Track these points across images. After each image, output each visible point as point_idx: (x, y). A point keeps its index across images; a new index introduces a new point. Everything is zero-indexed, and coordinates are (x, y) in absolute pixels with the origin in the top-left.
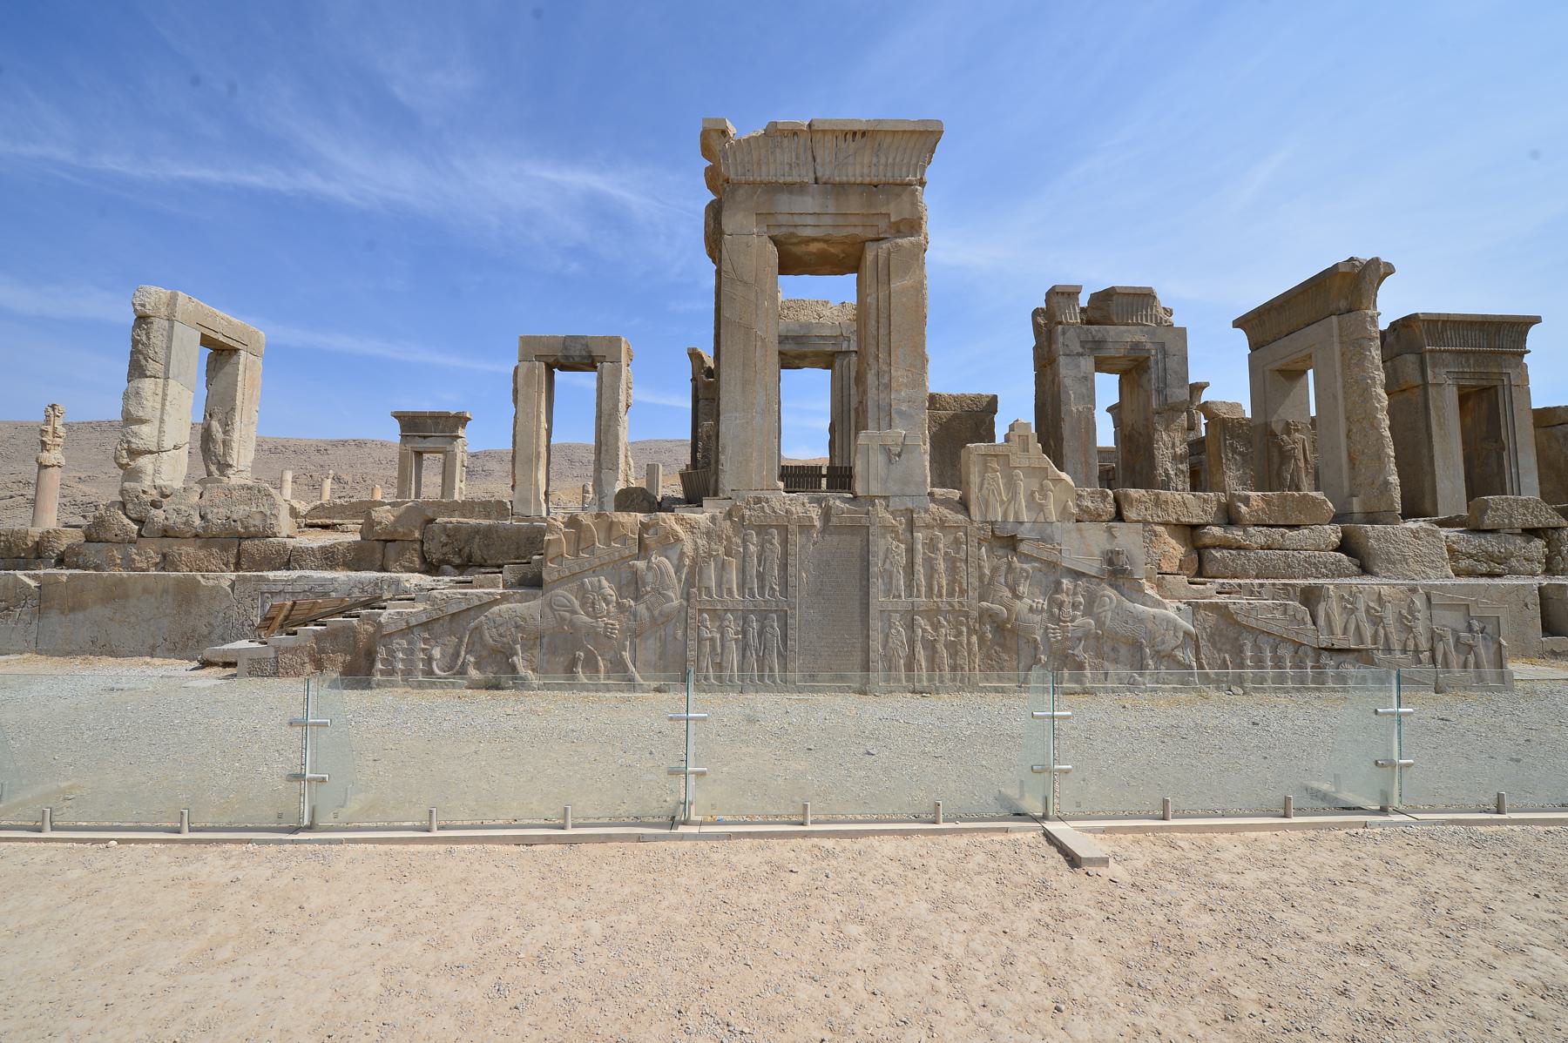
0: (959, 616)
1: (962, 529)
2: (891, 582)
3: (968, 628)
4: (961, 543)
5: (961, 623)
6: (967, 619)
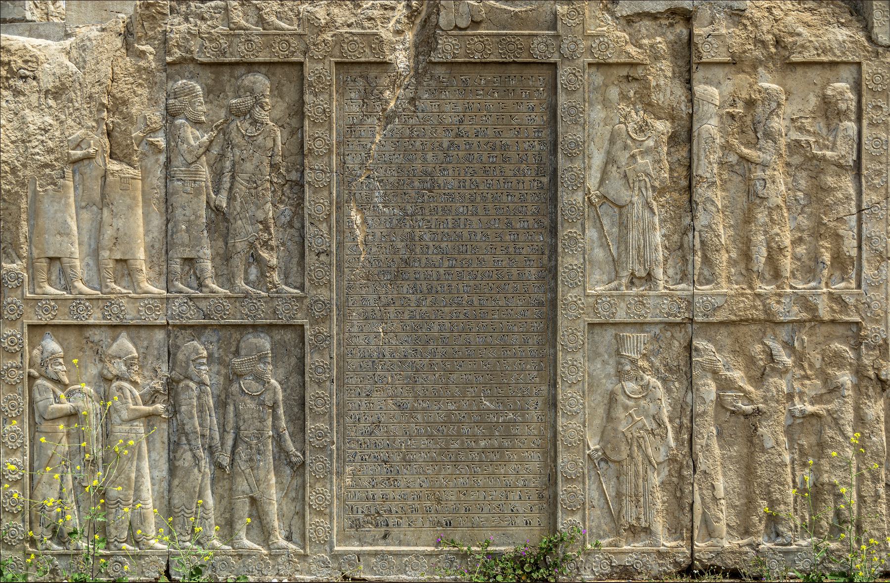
0: (829, 338)
1: (846, 72)
2: (622, 240)
3: (859, 372)
4: (841, 115)
5: (837, 360)
6: (856, 348)
